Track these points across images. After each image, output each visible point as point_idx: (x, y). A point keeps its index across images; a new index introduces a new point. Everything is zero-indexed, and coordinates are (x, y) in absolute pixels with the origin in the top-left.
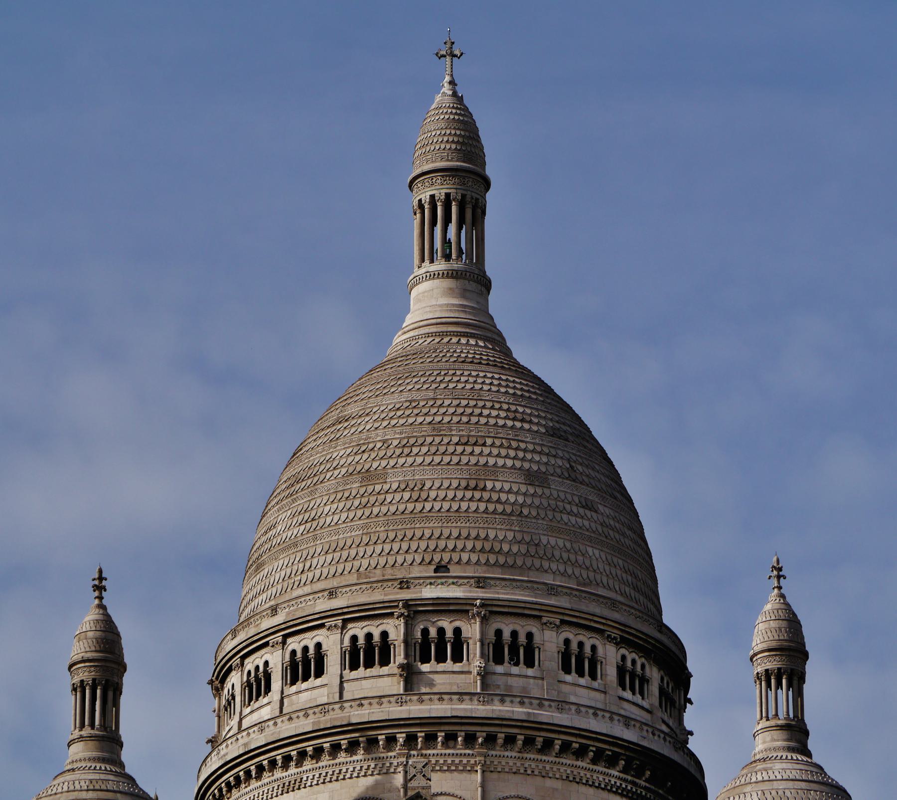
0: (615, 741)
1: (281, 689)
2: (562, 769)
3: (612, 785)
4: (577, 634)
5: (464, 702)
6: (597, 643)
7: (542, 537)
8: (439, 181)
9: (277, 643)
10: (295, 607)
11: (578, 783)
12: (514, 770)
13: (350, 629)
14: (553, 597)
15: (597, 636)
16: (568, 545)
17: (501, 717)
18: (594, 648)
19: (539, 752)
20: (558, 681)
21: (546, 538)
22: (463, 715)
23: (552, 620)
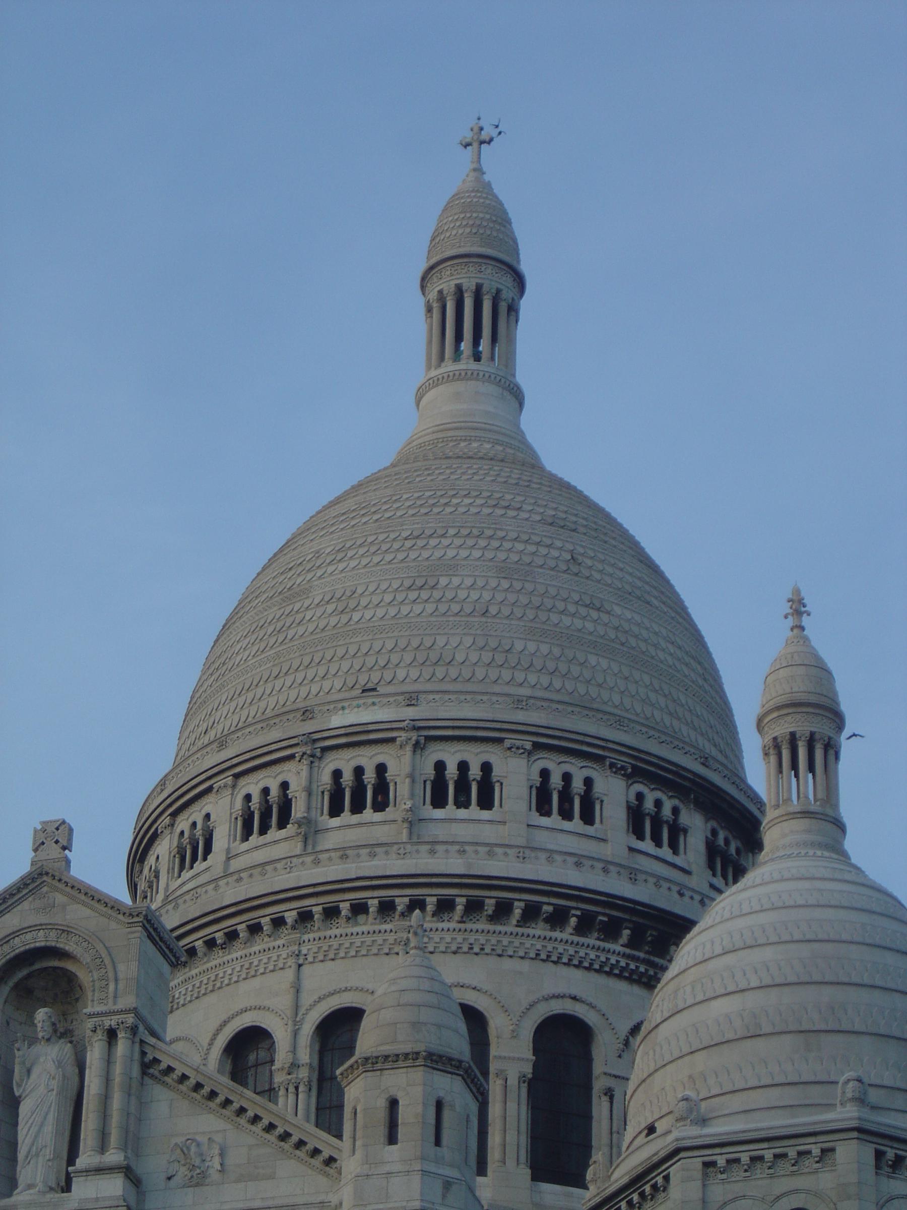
0: (610, 900)
2: (528, 943)
4: (560, 763)
5: (376, 858)
8: (448, 273)
11: (554, 962)
15: (594, 766)
18: (588, 782)
20: (528, 825)
22: (372, 874)
23: (518, 743)
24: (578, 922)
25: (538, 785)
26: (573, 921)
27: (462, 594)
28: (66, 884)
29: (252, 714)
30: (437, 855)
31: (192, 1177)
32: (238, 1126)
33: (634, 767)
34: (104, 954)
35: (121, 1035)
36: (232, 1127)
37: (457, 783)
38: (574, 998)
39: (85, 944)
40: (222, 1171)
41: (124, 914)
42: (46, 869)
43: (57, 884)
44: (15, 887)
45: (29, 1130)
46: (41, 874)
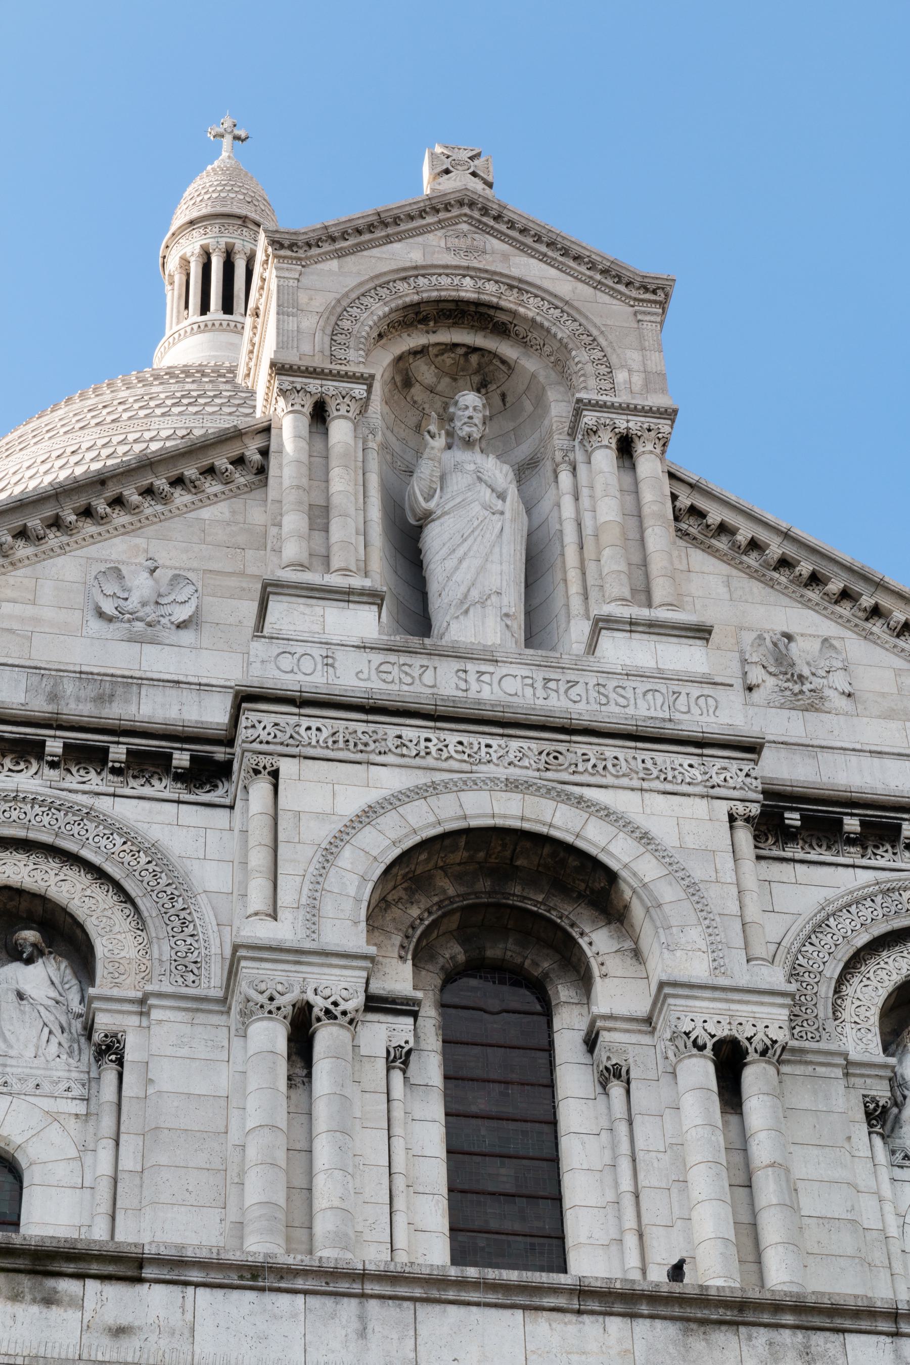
28: (511, 225)
32: (868, 636)
36: (854, 636)
39: (557, 313)
43: (492, 223)
44: (415, 207)
45: (460, 561)
46: (461, 203)
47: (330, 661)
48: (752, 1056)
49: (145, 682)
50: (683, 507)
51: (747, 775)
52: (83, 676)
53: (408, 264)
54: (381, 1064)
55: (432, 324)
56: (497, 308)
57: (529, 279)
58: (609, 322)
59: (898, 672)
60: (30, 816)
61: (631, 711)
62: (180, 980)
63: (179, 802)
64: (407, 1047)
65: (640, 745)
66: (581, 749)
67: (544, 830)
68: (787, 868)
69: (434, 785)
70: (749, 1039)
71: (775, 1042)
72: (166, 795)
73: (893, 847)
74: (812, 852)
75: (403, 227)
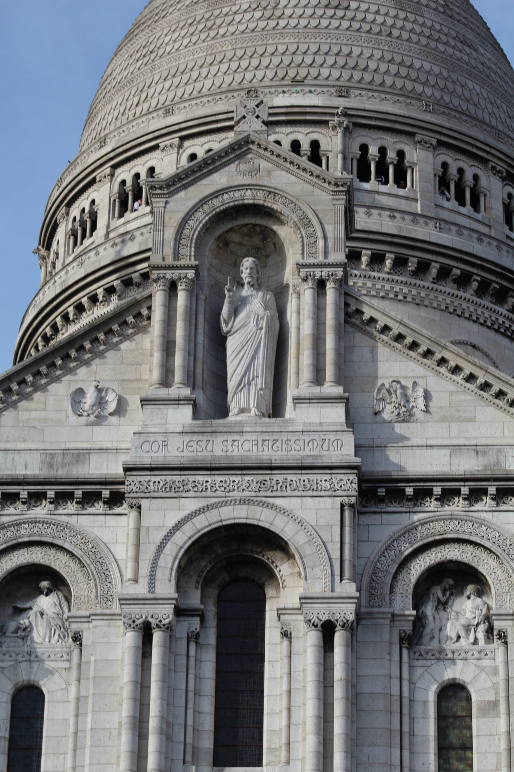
1: (107, 223)
2: (441, 298)
3: (500, 324)
4: (456, 159)
6: (480, 173)
7: (415, 61)
9: (105, 177)
10: (126, 133)
11: (459, 316)
12: (382, 294)
13: (188, 147)
14: (429, 114)
15: (480, 166)
16: (445, 73)
17: (367, 229)
18: (476, 177)
19: (412, 275)
20: (436, 205)
21: (420, 61)
23: (427, 139)
24: (479, 286)
25: (441, 174)
26: (475, 285)
27: (370, 17)
29: (188, 91)
30: (371, 217)
31: (399, 414)
33: (508, 171)
34: (311, 215)
35: (330, 285)
37: (377, 164)
38: (474, 346)
40: (427, 411)
41: (329, 183)
42: (252, 138)
43: (263, 152)
45: (240, 361)
47: (166, 443)
48: (338, 628)
49: (92, 451)
50: (351, 311)
51: (352, 482)
52: (65, 452)
53: (219, 188)
54: (185, 641)
55: (234, 215)
56: (263, 206)
57: (279, 187)
58: (318, 208)
59: (451, 393)
60: (42, 530)
61: (302, 453)
62: (105, 605)
63: (106, 515)
64: (196, 632)
65: (303, 472)
66: (275, 478)
67: (255, 522)
68: (378, 516)
69: (207, 506)
70: (337, 621)
71: (348, 621)
72: (101, 511)
73: (430, 499)
74: (392, 506)
75: (217, 164)
